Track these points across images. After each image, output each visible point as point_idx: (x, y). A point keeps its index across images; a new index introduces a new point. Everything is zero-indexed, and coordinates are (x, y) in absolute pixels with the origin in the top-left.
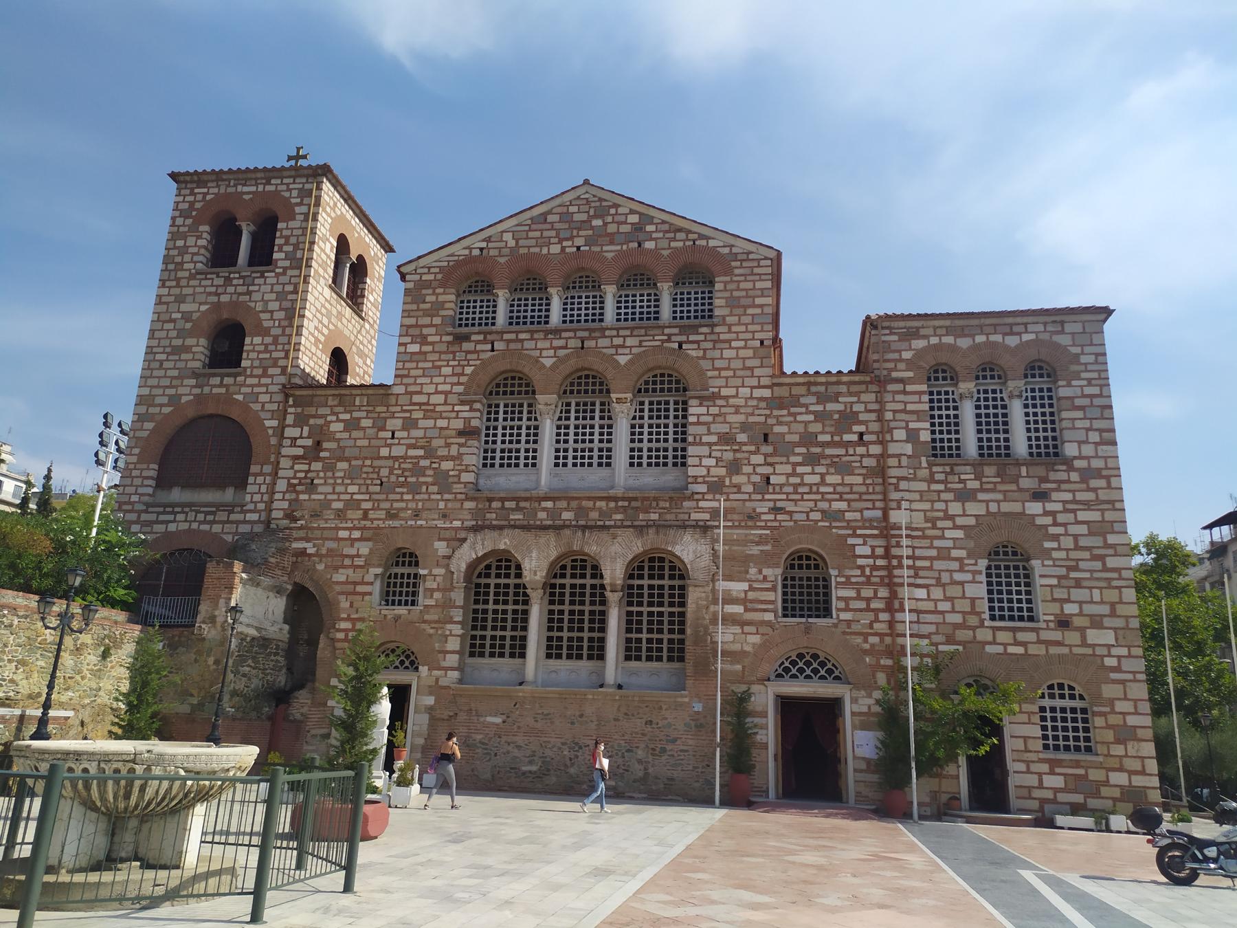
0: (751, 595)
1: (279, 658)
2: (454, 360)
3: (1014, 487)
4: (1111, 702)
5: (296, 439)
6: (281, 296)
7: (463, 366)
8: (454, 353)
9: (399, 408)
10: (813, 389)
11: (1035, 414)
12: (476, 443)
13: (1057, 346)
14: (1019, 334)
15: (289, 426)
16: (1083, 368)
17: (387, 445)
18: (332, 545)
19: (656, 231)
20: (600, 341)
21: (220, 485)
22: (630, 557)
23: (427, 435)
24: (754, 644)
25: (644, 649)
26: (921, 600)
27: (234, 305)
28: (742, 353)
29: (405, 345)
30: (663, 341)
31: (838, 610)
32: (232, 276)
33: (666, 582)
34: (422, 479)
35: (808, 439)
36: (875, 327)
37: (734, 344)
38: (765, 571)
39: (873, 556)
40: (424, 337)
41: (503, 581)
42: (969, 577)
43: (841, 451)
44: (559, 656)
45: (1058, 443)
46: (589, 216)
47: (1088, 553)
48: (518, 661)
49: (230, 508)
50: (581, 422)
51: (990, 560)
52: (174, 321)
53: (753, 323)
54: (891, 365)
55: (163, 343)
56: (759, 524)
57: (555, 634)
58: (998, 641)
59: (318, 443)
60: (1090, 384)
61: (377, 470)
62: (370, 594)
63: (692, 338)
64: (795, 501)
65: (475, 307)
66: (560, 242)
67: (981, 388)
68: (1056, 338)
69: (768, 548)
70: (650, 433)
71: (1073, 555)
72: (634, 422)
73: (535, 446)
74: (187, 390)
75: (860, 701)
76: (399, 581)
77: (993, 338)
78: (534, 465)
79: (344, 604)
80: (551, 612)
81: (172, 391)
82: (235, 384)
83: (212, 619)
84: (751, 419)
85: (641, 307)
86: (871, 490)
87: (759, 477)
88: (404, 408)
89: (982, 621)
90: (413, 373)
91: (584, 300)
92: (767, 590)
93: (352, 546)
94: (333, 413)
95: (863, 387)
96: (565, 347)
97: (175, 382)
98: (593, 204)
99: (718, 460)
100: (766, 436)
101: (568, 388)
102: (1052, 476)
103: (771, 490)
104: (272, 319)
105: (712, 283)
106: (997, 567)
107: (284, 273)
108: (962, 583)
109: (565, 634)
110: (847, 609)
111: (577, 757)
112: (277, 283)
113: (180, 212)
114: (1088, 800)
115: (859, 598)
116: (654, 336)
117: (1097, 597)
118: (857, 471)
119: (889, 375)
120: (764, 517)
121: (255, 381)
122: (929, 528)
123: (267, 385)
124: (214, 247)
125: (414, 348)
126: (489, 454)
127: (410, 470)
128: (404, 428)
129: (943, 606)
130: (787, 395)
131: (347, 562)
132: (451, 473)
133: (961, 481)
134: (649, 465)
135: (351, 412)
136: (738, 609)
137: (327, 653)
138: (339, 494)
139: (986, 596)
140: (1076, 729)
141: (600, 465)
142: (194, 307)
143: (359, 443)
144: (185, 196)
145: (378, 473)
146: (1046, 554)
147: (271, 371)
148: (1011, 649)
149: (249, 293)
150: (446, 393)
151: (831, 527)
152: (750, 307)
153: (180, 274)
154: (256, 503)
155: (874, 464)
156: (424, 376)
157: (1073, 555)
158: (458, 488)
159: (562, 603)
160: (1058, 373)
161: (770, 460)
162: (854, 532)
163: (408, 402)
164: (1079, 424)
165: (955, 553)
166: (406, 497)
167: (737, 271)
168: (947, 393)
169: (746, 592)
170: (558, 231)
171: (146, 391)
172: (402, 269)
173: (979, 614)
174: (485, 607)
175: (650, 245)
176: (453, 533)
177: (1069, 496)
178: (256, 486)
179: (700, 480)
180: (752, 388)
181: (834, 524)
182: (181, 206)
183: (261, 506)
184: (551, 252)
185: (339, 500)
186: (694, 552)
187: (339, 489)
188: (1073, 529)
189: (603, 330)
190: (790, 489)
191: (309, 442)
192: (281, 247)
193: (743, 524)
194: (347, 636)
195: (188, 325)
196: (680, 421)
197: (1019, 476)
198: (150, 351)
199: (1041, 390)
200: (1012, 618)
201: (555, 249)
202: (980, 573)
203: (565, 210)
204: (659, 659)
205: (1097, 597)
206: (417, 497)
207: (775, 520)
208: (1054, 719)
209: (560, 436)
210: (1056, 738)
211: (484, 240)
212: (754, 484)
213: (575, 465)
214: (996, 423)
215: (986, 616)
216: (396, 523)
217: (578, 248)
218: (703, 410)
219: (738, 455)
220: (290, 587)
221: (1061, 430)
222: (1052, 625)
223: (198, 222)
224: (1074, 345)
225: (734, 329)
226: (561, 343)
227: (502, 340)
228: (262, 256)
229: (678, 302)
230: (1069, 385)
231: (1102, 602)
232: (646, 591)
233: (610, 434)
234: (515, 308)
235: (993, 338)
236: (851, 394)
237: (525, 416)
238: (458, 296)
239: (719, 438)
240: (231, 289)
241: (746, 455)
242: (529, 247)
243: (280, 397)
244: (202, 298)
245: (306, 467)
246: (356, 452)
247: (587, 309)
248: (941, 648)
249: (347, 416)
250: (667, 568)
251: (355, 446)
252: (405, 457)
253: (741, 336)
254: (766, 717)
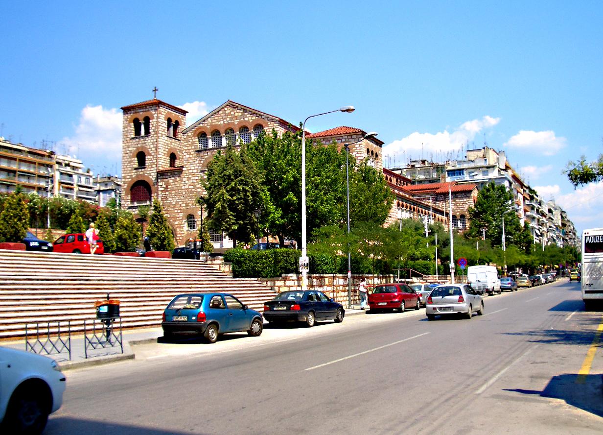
6: (153, 143)
18: (174, 214)
27: (142, 147)
40: (190, 153)
59: (167, 186)
79: (178, 230)
81: (130, 174)
125: (188, 156)
131: (178, 219)
147: (153, 166)
149: (145, 143)
166: (190, 200)
167: (269, 126)
170: (222, 116)
175: (246, 119)
191: (165, 186)
201: (222, 122)
223: (130, 122)
228: (147, 132)
238: (198, 138)
240: (140, 142)
242: (215, 122)
244: (134, 146)
245: (164, 193)
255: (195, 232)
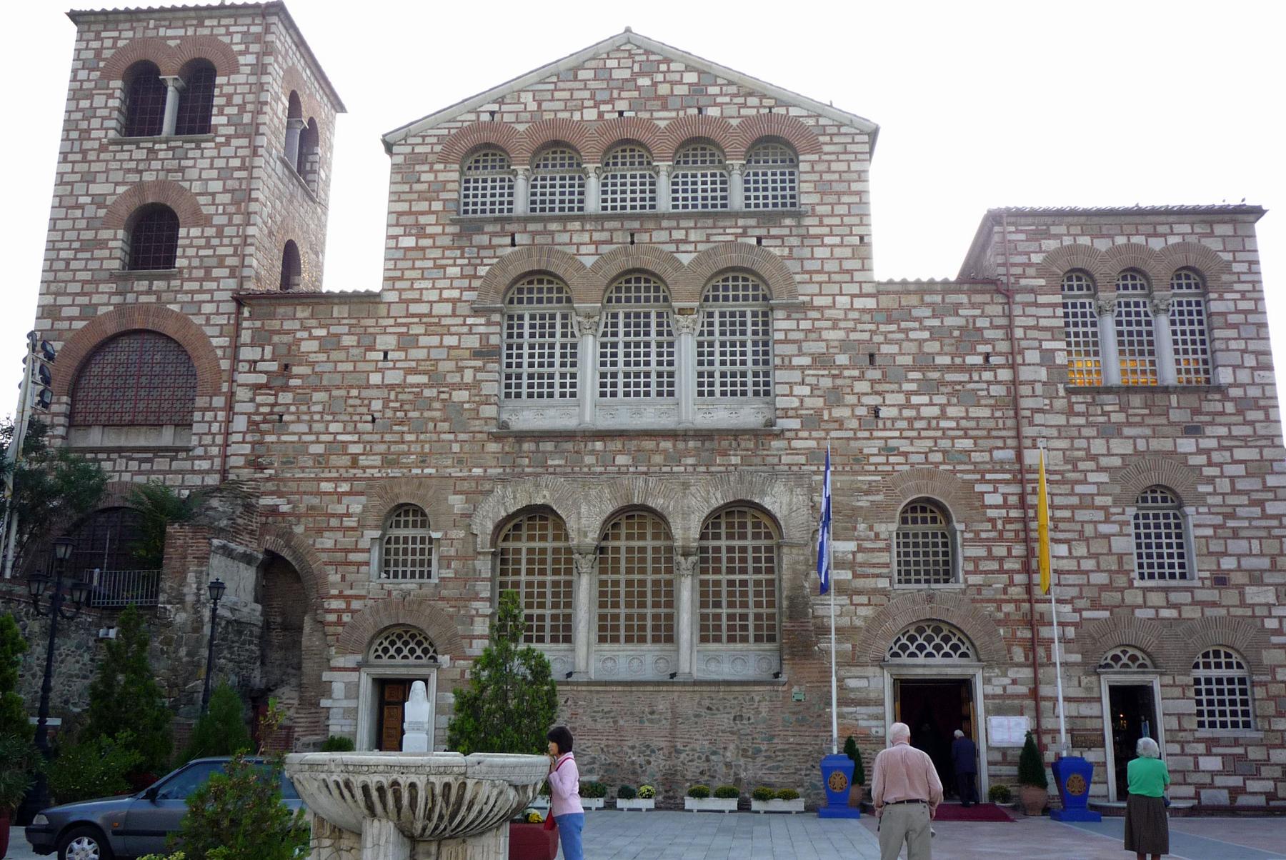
0: (860, 557)
1: (253, 647)
2: (462, 257)
3: (1163, 420)
4: (1273, 669)
5: (255, 362)
7: (476, 266)
8: (461, 248)
9: (391, 321)
10: (928, 299)
11: (1183, 333)
12: (495, 366)
13: (1206, 252)
14: (1164, 235)
15: (245, 345)
16: (1235, 278)
17: (378, 370)
19: (721, 94)
20: (654, 233)
21: (158, 425)
22: (707, 512)
23: (432, 356)
24: (865, 618)
25: (724, 627)
26: (1063, 558)
27: (161, 185)
28: (838, 252)
29: (396, 237)
30: (737, 235)
31: (967, 572)
32: (157, 146)
33: (749, 543)
34: (427, 414)
35: (923, 363)
36: (1000, 224)
37: (827, 240)
38: (877, 527)
39: (1005, 505)
40: (423, 227)
41: (537, 544)
42: (1114, 528)
43: (965, 377)
44: (615, 639)
45: (1210, 366)
46: (633, 72)
47: (1246, 498)
48: (563, 646)
49: (173, 452)
50: (632, 338)
51: (1139, 508)
52: (82, 207)
53: (849, 215)
54: (1019, 271)
55: (69, 235)
56: (867, 468)
57: (610, 611)
58: (1149, 604)
59: (286, 367)
60: (1243, 298)
61: (366, 402)
62: (367, 564)
63: (774, 231)
64: (911, 439)
65: (484, 188)
66: (596, 105)
67: (1123, 300)
68: (1207, 242)
69: (880, 498)
70: (723, 354)
71: (1232, 500)
72: (701, 338)
73: (573, 370)
74: (104, 298)
75: (995, 681)
76: (401, 546)
77: (1135, 240)
78: (573, 395)
79: (334, 578)
80: (603, 583)
81: (85, 300)
82: (168, 290)
83: (179, 599)
84: (853, 336)
85: (704, 191)
86: (1001, 425)
87: (865, 409)
88: (399, 320)
89: (1131, 581)
90: (408, 274)
91: (629, 180)
92: (880, 550)
93: (340, 502)
94: (304, 328)
95: (987, 298)
96: (610, 242)
97: (88, 288)
98: (637, 58)
99: (814, 388)
100: (872, 356)
101: (614, 295)
102: (1207, 407)
103: (881, 425)
104: (213, 204)
105: (794, 162)
106: (1146, 517)
107: (227, 144)
108: (1107, 537)
109: (623, 611)
110: (976, 572)
111: (649, 763)
112: (219, 157)
113: (82, 63)
114: (1248, 782)
115: (990, 557)
116: (725, 228)
117: (1256, 550)
118: (983, 402)
119: (1017, 282)
120: (872, 460)
121: (196, 286)
122: (1069, 471)
123: (211, 292)
124: (128, 109)
125: (409, 242)
126: (513, 381)
127: (411, 402)
128: (399, 349)
129: (1088, 564)
130: (896, 306)
131: (334, 522)
132: (466, 406)
133: (1104, 413)
134: (724, 394)
135: (327, 326)
136: (846, 575)
137: (317, 642)
138: (318, 434)
139: (1135, 551)
140: (1233, 703)
141: (660, 394)
142: (107, 188)
143: (341, 367)
144: (88, 41)
145: (369, 406)
146: (1200, 499)
147: (216, 273)
148: (1165, 613)
149: (181, 169)
150: (454, 301)
151: (954, 472)
152: (844, 193)
153: (87, 145)
154: (205, 446)
155: (1004, 393)
156: (423, 278)
157: (1232, 500)
158: (477, 425)
159: (616, 570)
160: (1209, 283)
161: (878, 387)
162: (983, 476)
163: (403, 314)
164: (1233, 345)
165: (1099, 501)
167: (826, 148)
168: (1083, 306)
169: (854, 553)
171: (49, 300)
172: (389, 139)
173: (1128, 572)
174: (516, 578)
175: (713, 112)
176: (473, 485)
177: (1223, 431)
178: (206, 424)
179: (791, 413)
180: (853, 296)
181: (958, 468)
182: (84, 55)
183: (215, 451)
184: (585, 118)
185: (318, 442)
186: (790, 504)
187: (318, 427)
188: (1231, 470)
189: (658, 217)
190: (904, 424)
191: (274, 367)
192: (221, 109)
193: (848, 468)
194: (340, 618)
195: (102, 212)
196: (760, 337)
197: (1169, 407)
198: (52, 246)
199: (1189, 304)
200: (1162, 576)
201: (591, 114)
202: (1128, 523)
203: (601, 64)
204: (744, 639)
205: (1256, 550)
206: (422, 437)
207: (887, 463)
208: (1209, 692)
209: (607, 355)
210: (1211, 714)
211: (495, 102)
212: (860, 418)
213: (627, 394)
214: (1140, 343)
215: (1136, 575)
216: (396, 473)
217: (621, 113)
218: (790, 324)
219: (839, 382)
220: (261, 556)
221: (1213, 352)
222: (1208, 583)
224: (1225, 250)
225: (826, 221)
226: (604, 236)
227: (525, 231)
229: (752, 186)
230: (1221, 298)
231: (1262, 555)
232: (724, 555)
233: (671, 354)
234: (539, 190)
235: (1135, 240)
236: (973, 306)
237: (558, 330)
238: (462, 173)
239: (814, 360)
240: (156, 165)
241: (848, 381)
242: (555, 110)
243: (231, 307)
244: (119, 176)
245: (271, 399)
246: (337, 379)
247: (633, 192)
248: (1086, 614)
249: (323, 332)
250: (749, 525)
251: (336, 371)
252: (403, 386)
253: (836, 230)
254: (883, 704)
255: (425, 590)
